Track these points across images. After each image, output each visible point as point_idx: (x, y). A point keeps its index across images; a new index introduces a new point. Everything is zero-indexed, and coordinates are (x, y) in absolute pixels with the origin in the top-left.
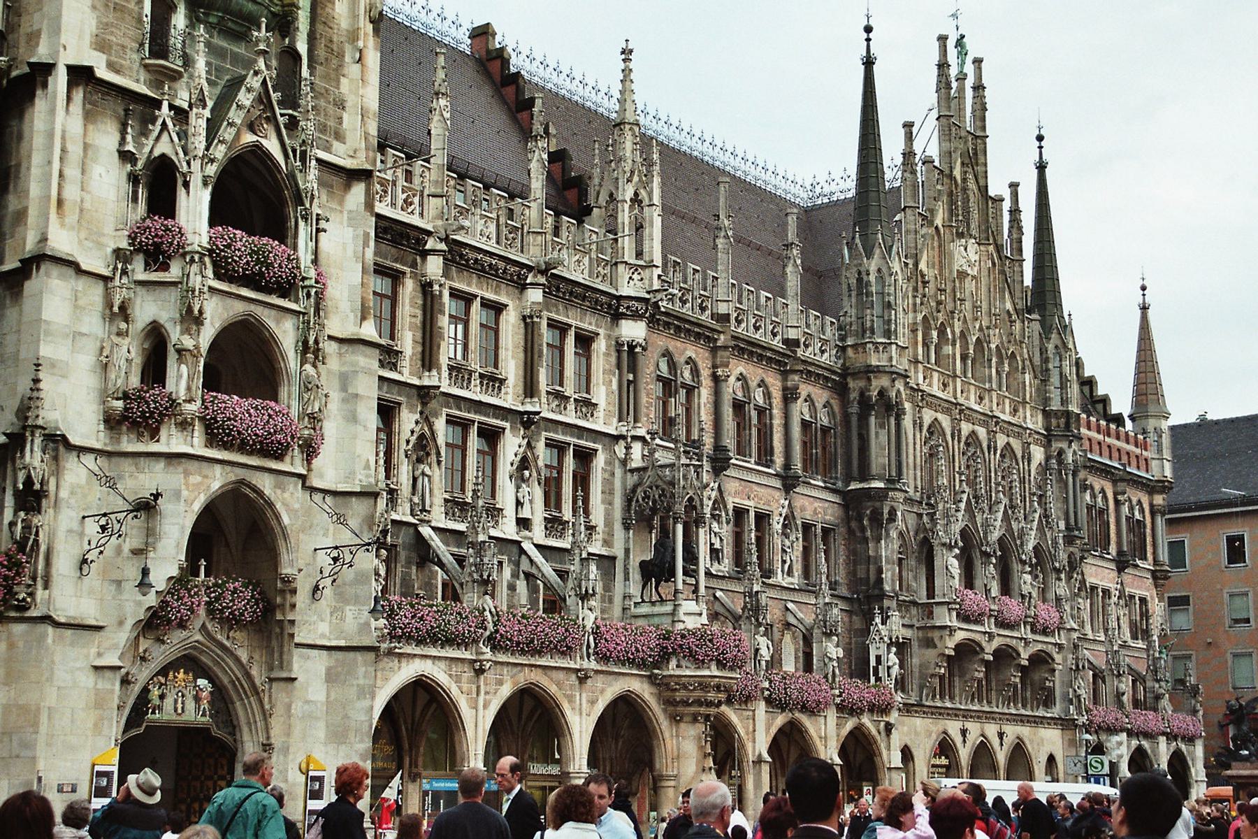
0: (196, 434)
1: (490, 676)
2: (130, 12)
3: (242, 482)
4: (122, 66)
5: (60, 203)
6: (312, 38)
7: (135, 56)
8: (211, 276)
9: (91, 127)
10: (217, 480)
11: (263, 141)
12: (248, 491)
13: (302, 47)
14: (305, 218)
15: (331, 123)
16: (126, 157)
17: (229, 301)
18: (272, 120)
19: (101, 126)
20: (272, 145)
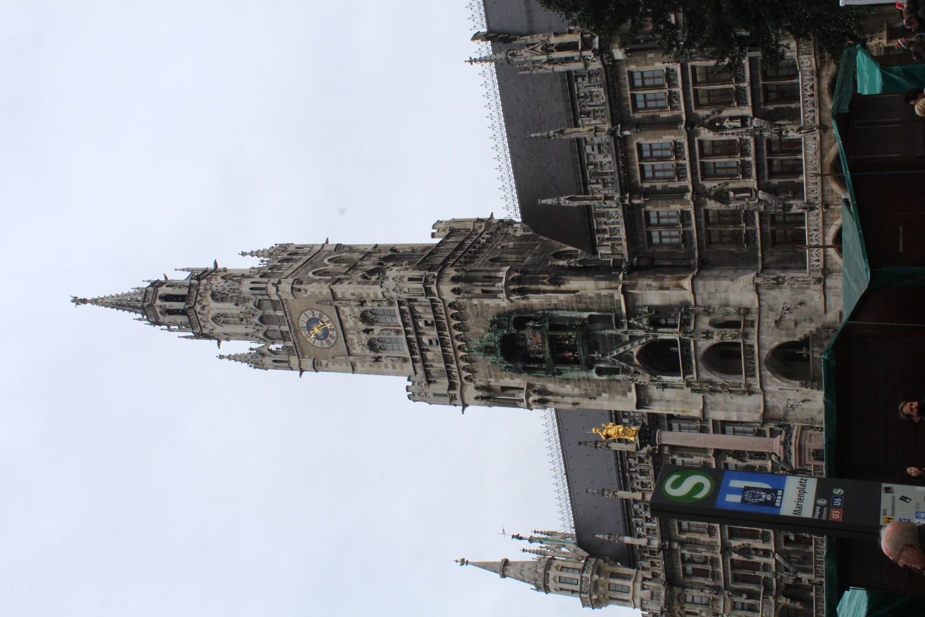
1: (829, 198)
3: (766, 362)
11: (635, 354)
13: (586, 315)
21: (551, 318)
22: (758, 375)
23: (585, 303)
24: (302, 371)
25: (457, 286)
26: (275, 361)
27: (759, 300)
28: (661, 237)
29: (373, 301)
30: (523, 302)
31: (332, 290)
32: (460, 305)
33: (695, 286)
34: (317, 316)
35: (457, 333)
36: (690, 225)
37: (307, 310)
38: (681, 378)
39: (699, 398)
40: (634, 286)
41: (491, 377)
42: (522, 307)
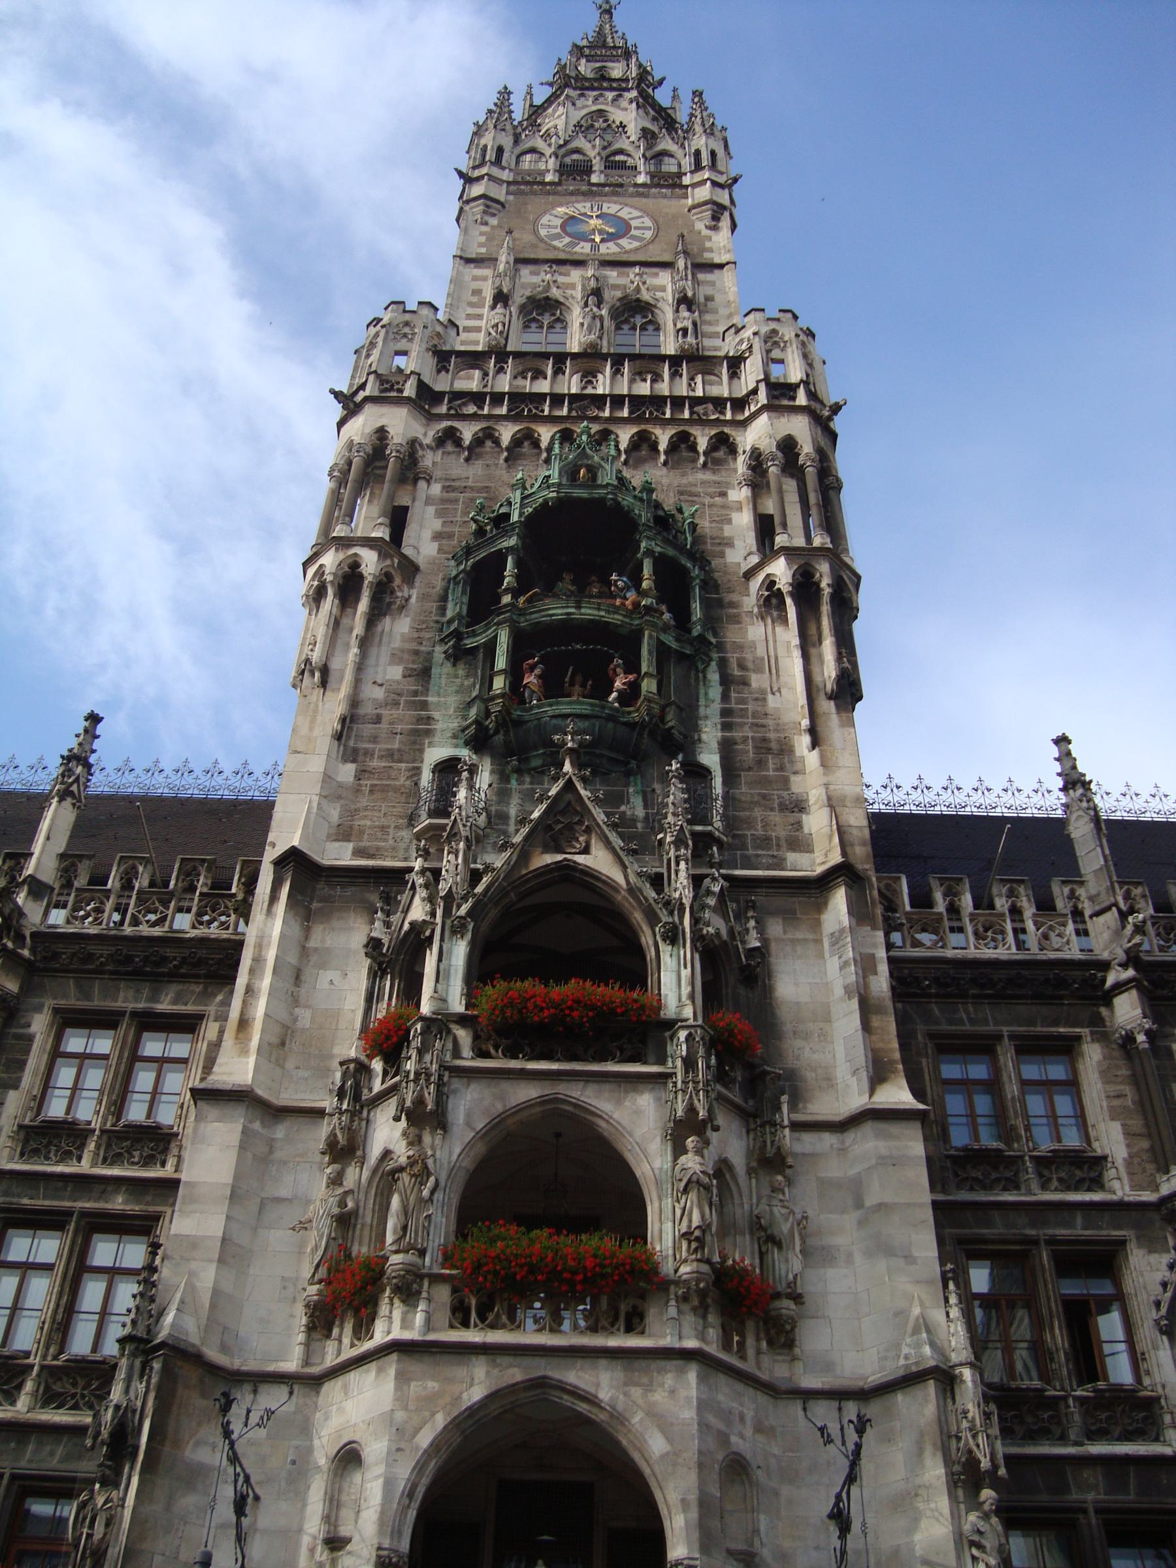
0: (422, 1306)
2: (396, 790)
3: (541, 1383)
4: (378, 849)
6: (727, 749)
7: (406, 834)
8: (467, 1052)
10: (476, 1384)
11: (580, 859)
12: (567, 1400)
13: (710, 759)
14: (673, 936)
15: (780, 832)
16: (373, 945)
17: (506, 1086)
19: (336, 924)
20: (598, 859)
22: (473, 1336)
23: (761, 763)
24: (468, 180)
26: (500, 150)
27: (839, 1395)
29: (695, 324)
30: (750, 600)
31: (721, 266)
32: (718, 462)
33: (895, 1128)
34: (633, 232)
35: (625, 435)
36: (1044, 1187)
37: (655, 221)
40: (859, 912)
41: (446, 489)
42: (728, 597)
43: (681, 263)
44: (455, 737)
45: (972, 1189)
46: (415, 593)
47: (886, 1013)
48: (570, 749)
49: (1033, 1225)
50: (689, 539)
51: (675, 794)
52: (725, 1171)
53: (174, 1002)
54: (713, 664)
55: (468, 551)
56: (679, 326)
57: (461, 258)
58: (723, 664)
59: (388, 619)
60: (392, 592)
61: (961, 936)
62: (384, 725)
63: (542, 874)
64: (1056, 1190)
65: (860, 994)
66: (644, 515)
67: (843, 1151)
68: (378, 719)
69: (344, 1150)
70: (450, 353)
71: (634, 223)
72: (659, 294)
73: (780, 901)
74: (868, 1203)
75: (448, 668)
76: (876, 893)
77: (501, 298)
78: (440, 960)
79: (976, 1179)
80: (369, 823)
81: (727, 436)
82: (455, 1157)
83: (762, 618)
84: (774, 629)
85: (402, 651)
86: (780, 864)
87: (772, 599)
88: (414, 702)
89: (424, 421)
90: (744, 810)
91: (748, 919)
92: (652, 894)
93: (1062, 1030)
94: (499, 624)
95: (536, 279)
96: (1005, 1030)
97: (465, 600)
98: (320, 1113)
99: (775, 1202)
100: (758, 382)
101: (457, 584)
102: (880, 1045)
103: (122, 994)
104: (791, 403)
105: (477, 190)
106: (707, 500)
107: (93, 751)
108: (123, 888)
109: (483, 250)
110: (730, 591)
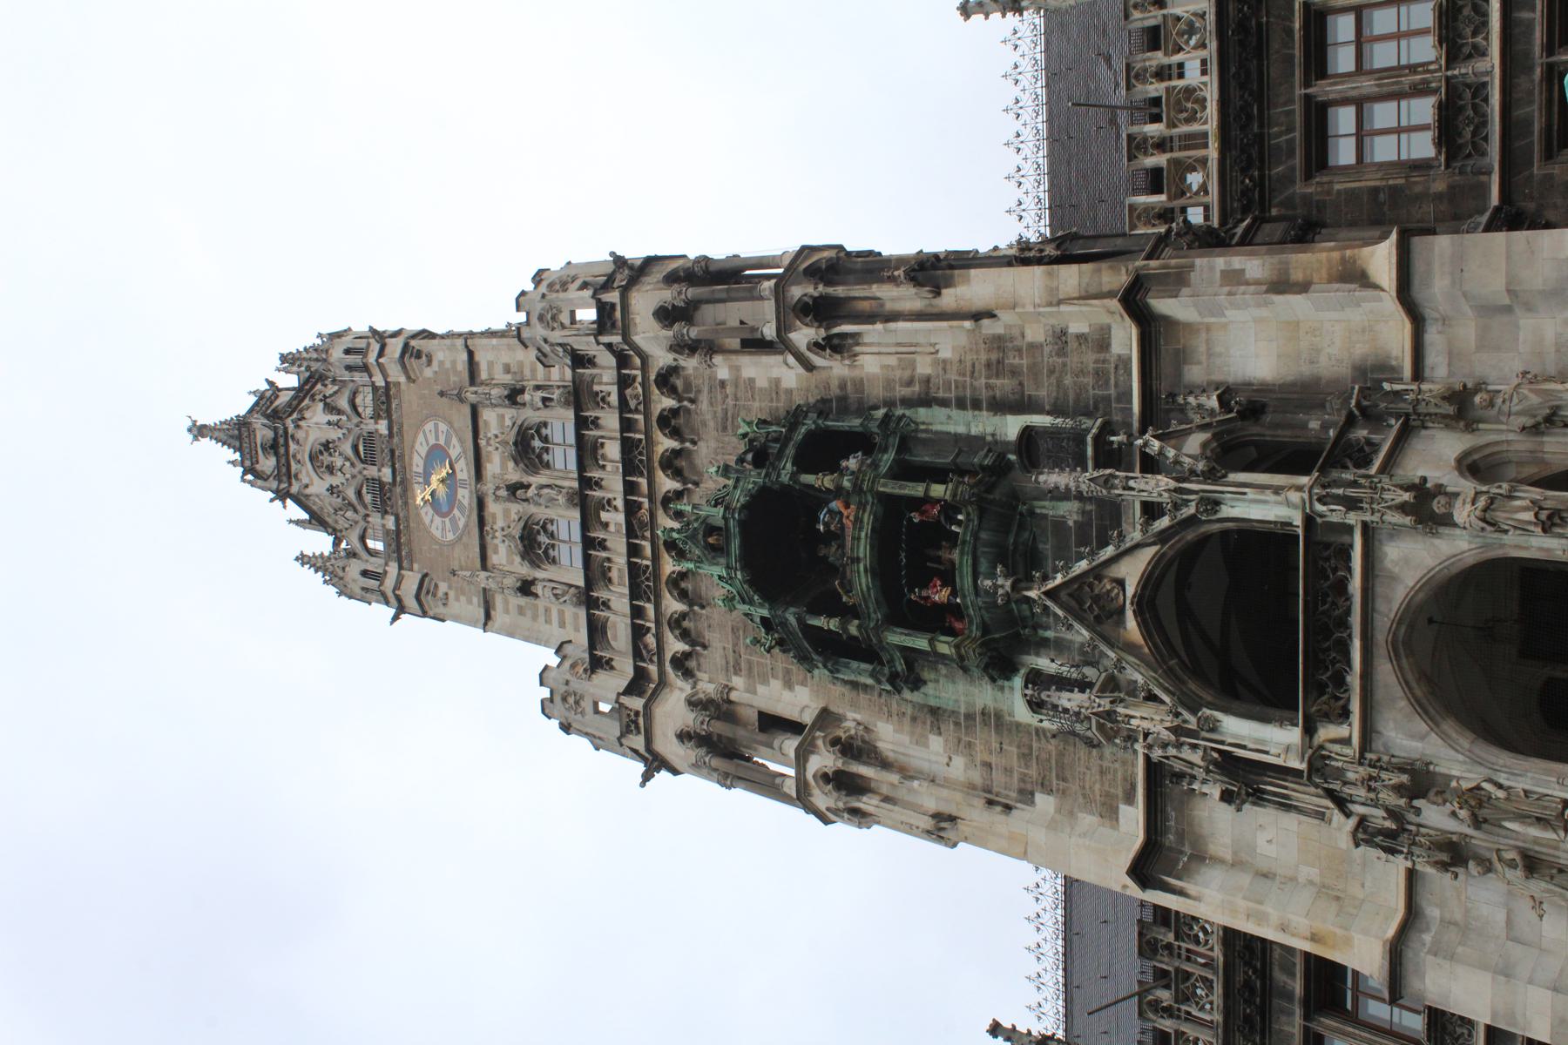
2: (1061, 754)
4: (1125, 779)
5: (1314, 938)
6: (1001, 406)
8: (1341, 731)
9: (1214, 849)
11: (1130, 590)
13: (1012, 427)
14: (1213, 504)
15: (1090, 358)
17: (1379, 694)
18: (1097, 573)
20: (1132, 571)
21: (906, 443)
23: (1015, 372)
24: (401, 609)
25: (667, 295)
26: (365, 573)
28: (1362, 134)
29: (538, 388)
30: (835, 369)
31: (471, 354)
32: (688, 386)
33: (1418, 266)
34: (442, 442)
36: (1481, 52)
38: (1294, 735)
39: (1385, 878)
41: (737, 670)
42: (835, 391)
43: (472, 398)
44: (1002, 689)
45: (1486, 139)
46: (850, 715)
47: (1287, 263)
48: (1013, 586)
49: (1531, 69)
50: (774, 428)
51: (1053, 478)
52: (1470, 460)
53: (1292, 975)
54: (908, 413)
55: (803, 659)
56: (540, 404)
57: (485, 624)
58: (908, 403)
59: (880, 745)
60: (851, 737)
61: (1187, 66)
62: (993, 760)
63: (1148, 631)
64: (1486, 39)
65: (1267, 292)
66: (755, 479)
67: (1445, 320)
68: (988, 765)
69: (1454, 855)
70: (592, 656)
71: (432, 441)
72: (508, 423)
73: (1165, 366)
74: (1507, 301)
75: (929, 689)
76: (1153, 263)
77: (526, 588)
78: (1244, 747)
79: (1474, 134)
80: (1097, 786)
81: (659, 375)
82: (1461, 758)
83: (855, 355)
84: (865, 344)
85: (912, 734)
86: (1124, 362)
87: (836, 346)
88: (967, 727)
89: (667, 690)
90: (1066, 394)
91: (1187, 403)
92: (1164, 522)
93: (1297, 26)
94: (880, 641)
95: (502, 549)
96: (1299, 92)
97: (855, 664)
98: (1412, 876)
99: (1505, 408)
100: (598, 343)
101: (838, 671)
102: (1324, 273)
103: (1286, 1028)
104: (618, 308)
105: (410, 602)
106: (730, 402)
107: (1029, 1033)
108: (1171, 1016)
109: (475, 600)
110: (827, 386)
